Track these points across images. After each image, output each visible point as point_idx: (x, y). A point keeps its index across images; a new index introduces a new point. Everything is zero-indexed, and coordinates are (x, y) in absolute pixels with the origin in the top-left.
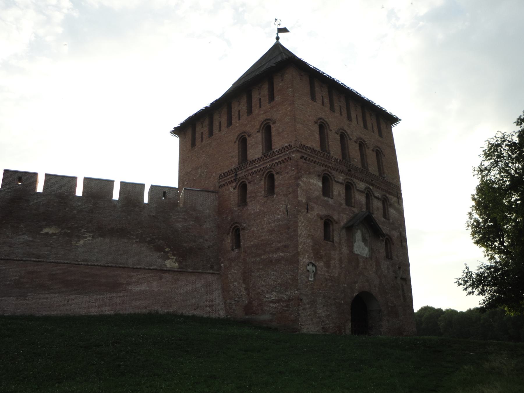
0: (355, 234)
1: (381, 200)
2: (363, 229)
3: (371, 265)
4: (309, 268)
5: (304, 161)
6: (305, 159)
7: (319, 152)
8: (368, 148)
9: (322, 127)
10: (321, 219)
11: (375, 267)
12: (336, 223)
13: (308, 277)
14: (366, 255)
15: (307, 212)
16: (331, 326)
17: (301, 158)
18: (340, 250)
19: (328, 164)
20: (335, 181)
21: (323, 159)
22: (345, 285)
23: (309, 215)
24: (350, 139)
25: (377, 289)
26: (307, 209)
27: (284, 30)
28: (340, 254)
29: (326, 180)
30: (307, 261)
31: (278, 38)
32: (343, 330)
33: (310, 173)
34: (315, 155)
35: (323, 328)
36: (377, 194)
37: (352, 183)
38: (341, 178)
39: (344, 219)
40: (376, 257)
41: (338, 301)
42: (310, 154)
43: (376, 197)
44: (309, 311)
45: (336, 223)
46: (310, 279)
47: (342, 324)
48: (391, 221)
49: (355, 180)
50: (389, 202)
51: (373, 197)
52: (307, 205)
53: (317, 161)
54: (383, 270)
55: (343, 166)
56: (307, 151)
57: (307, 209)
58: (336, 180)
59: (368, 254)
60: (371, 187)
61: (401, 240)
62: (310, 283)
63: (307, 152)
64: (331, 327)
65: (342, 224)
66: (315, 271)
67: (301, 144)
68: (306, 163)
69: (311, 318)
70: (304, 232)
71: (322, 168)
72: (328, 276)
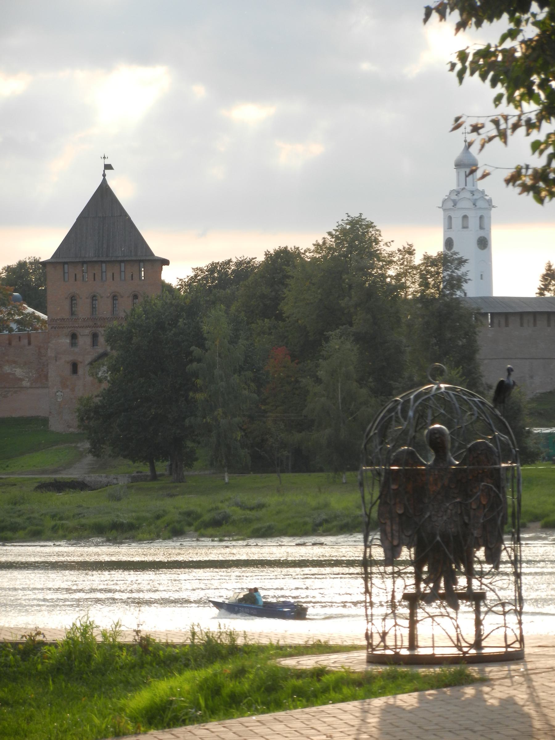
4: (57, 394)
6: (55, 328)
8: (122, 297)
9: (73, 299)
10: (68, 363)
12: (81, 363)
17: (52, 328)
23: (57, 363)
24: (102, 297)
26: (56, 360)
27: (108, 167)
29: (74, 337)
31: (104, 175)
35: (68, 426)
38: (87, 331)
39: (89, 359)
45: (81, 363)
46: (59, 400)
57: (56, 360)
58: (82, 334)
65: (87, 362)
71: (69, 330)
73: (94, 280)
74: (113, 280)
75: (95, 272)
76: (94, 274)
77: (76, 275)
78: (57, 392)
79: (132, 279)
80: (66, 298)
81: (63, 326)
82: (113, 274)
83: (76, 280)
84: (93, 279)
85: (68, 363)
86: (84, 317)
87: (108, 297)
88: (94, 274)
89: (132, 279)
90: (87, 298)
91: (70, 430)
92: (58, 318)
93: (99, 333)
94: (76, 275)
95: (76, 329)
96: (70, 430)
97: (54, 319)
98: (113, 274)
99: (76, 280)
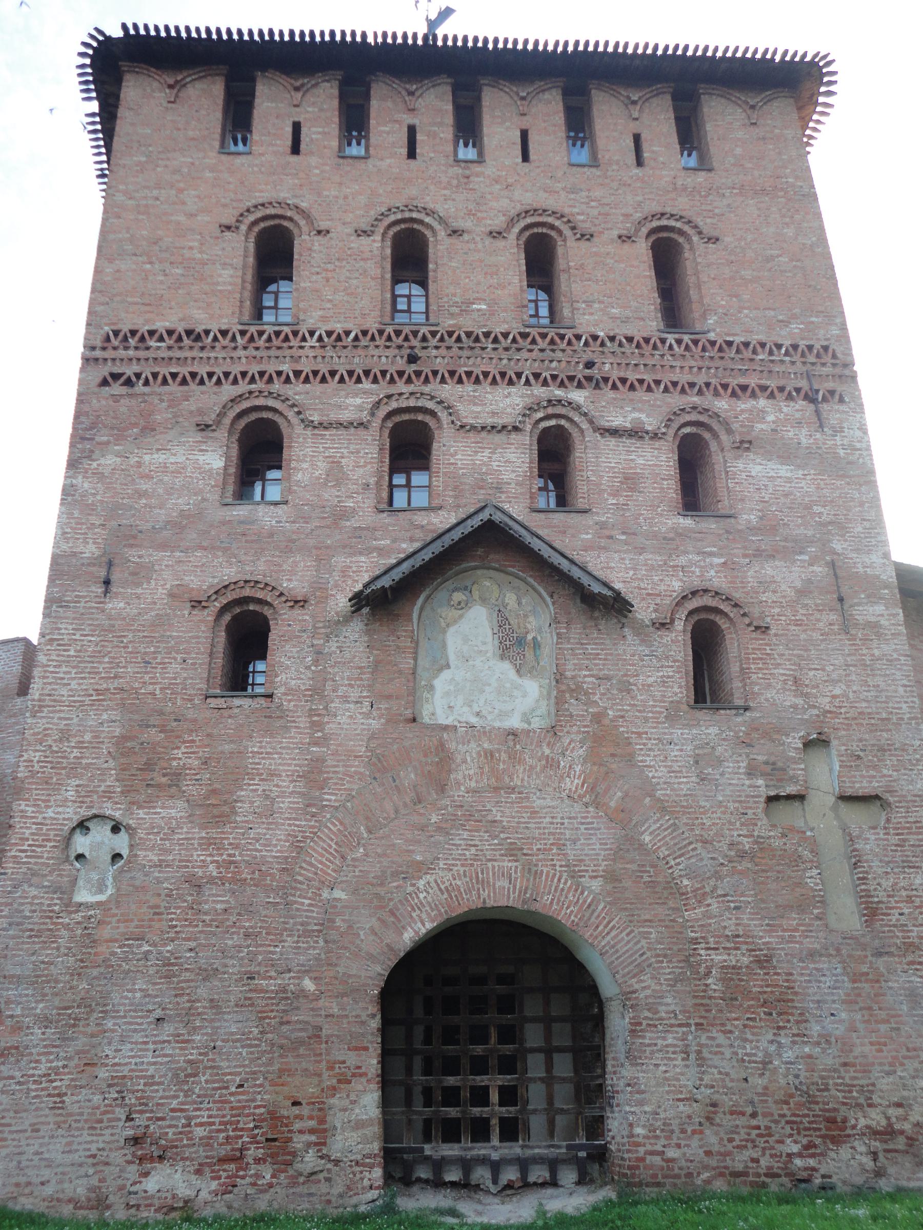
0: (444, 632)
1: (655, 436)
2: (511, 598)
3: (551, 763)
4: (81, 843)
5: (124, 390)
6: (128, 383)
7: (224, 333)
8: (586, 237)
10: (197, 604)
11: (578, 769)
12: (299, 603)
13: (65, 891)
14: (526, 719)
15: (106, 592)
16: (201, 1124)
17: (104, 383)
18: (316, 726)
19: (271, 368)
20: (309, 424)
21: (241, 353)
22: (338, 894)
23: (115, 605)
25: (596, 885)
28: (316, 744)
30: (72, 814)
32: (299, 1141)
33: (149, 429)
34: (196, 353)
35: (136, 1141)
36: (617, 421)
37: (430, 405)
40: (598, 718)
41: (271, 985)
42: (171, 354)
43: (614, 432)
44: (43, 1059)
45: (299, 603)
46: (83, 896)
47: (296, 1103)
48: (749, 517)
49: (448, 391)
50: (729, 431)
51: (590, 436)
52: (110, 564)
53: (203, 371)
54: (658, 774)
55: (372, 351)
56: (148, 348)
57: (107, 582)
58: (316, 418)
59: (543, 709)
60: (578, 396)
61: (841, 600)
62: (78, 917)
63: (150, 354)
64: (200, 1132)
66: (125, 852)
67: (116, 333)
68: (130, 396)
69: (49, 1095)
70: (74, 685)
71: (228, 391)
72: (212, 867)
73: (412, 154)
74: (525, 157)
75: (416, 121)
76: (412, 131)
77: (297, 128)
78: (82, 826)
79: (640, 162)
80: (228, 228)
81: (184, 371)
82: (524, 135)
83: (296, 149)
84: (404, 151)
85: (197, 604)
86: (339, 328)
87: (495, 234)
88: (412, 131)
89: (640, 162)
90: (361, 233)
91: (151, 1185)
92: (161, 325)
93: (443, 415)
94: (297, 128)
95: (277, 386)
96: (151, 1185)
97: (133, 333)
98: (524, 135)
99: (296, 149)
